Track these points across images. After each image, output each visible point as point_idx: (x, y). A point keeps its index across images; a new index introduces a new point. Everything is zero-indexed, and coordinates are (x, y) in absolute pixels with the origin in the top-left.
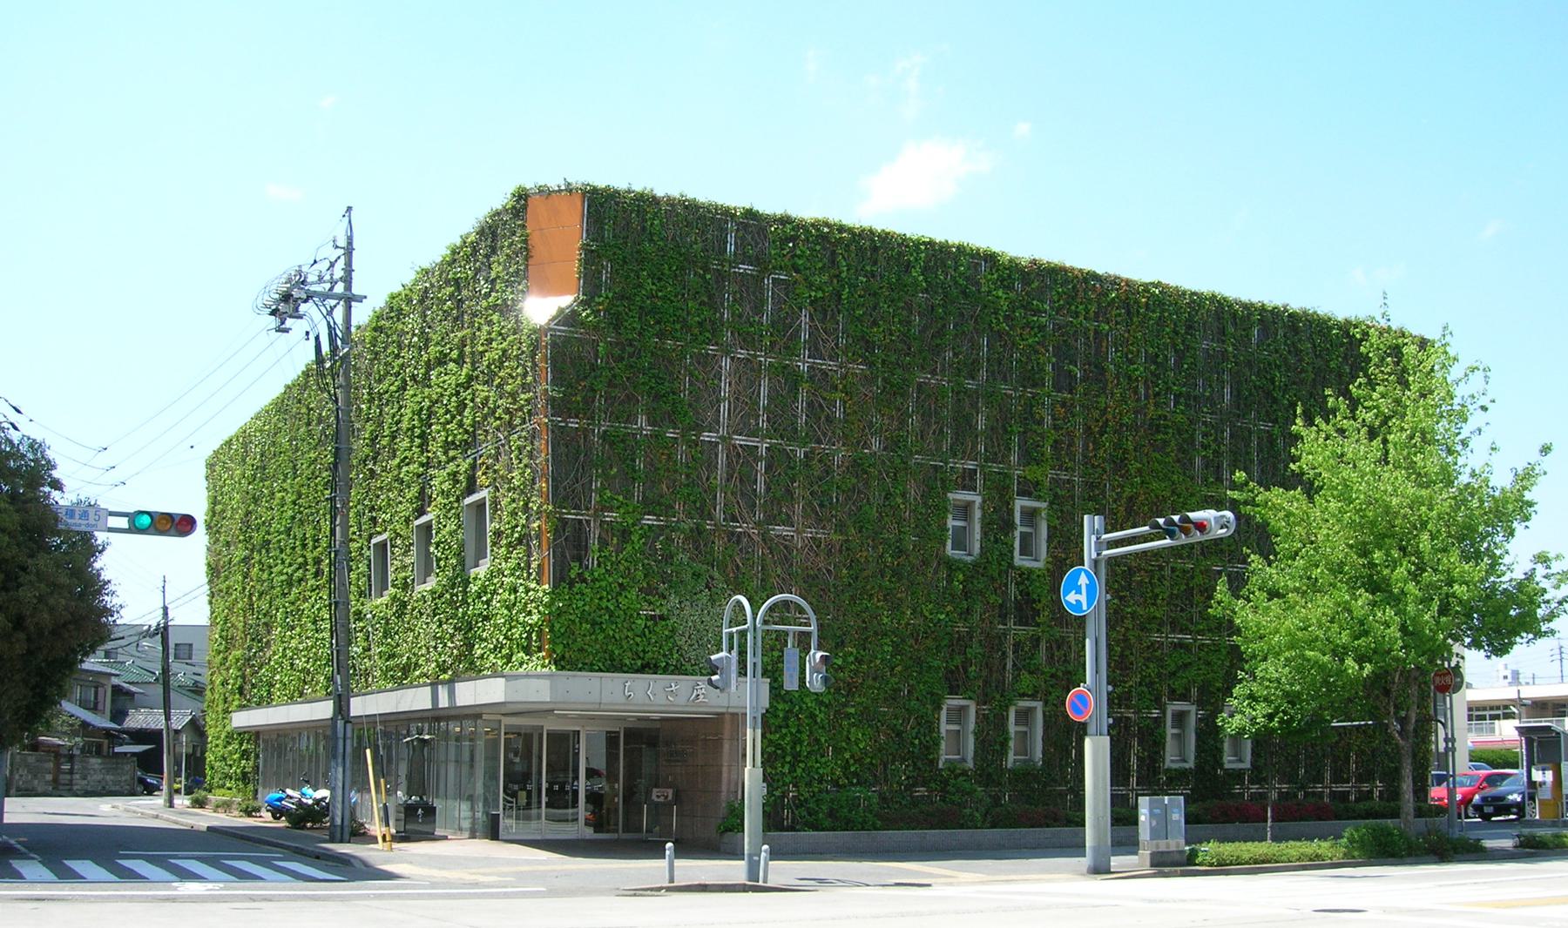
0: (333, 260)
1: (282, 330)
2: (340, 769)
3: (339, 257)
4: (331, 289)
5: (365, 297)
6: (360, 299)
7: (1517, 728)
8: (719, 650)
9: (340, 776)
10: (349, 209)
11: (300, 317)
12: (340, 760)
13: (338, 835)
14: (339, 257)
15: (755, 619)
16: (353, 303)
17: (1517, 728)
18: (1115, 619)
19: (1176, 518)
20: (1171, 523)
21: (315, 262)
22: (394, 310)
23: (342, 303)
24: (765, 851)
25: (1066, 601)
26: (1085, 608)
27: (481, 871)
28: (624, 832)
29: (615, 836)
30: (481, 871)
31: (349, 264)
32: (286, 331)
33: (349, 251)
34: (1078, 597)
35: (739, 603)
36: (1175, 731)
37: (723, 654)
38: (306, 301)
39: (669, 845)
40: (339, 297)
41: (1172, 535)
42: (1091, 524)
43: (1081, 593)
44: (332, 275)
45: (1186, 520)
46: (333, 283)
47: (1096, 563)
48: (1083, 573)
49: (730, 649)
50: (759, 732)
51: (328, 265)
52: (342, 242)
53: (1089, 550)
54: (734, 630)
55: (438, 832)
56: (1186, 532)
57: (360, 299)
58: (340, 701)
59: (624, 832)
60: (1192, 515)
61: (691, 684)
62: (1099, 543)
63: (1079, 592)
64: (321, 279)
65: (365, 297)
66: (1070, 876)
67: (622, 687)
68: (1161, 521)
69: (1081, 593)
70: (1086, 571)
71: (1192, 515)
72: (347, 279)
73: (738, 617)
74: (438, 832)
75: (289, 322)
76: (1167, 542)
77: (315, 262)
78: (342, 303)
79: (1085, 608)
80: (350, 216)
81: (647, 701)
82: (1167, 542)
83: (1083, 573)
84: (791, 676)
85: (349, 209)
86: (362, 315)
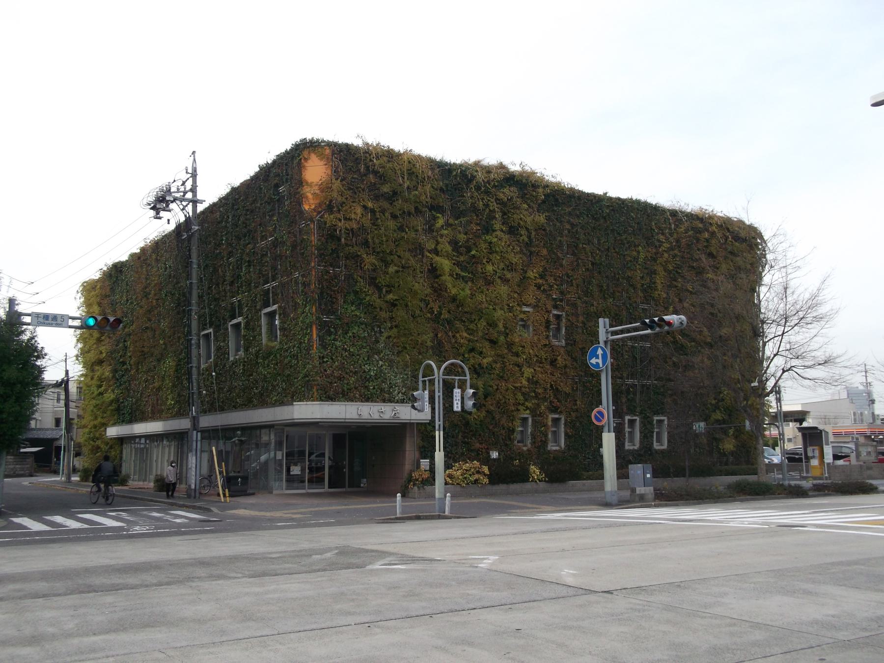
0: (184, 180)
1: (157, 217)
2: (194, 458)
3: (188, 179)
4: (184, 196)
5: (205, 201)
6: (202, 202)
7: (798, 428)
8: (417, 390)
9: (194, 461)
10: (194, 153)
11: (170, 211)
12: (194, 453)
13: (193, 494)
14: (188, 179)
15: (439, 374)
16: (198, 204)
17: (798, 428)
18: (616, 369)
19: (656, 319)
20: (653, 321)
21: (175, 181)
22: (213, 208)
23: (191, 204)
24: (449, 496)
25: (590, 363)
26: (601, 366)
27: (292, 511)
28: (349, 487)
29: (344, 490)
30: (292, 511)
31: (194, 182)
32: (160, 218)
33: (194, 175)
34: (597, 360)
35: (429, 366)
36: (630, 430)
37: (419, 392)
38: (172, 202)
39: (399, 495)
40: (190, 201)
41: (652, 328)
42: (603, 323)
43: (598, 359)
44: (185, 188)
45: (661, 320)
46: (185, 193)
47: (606, 342)
48: (599, 349)
49: (424, 389)
50: (442, 433)
51: (182, 182)
52: (190, 171)
53: (602, 337)
54: (426, 379)
55: (249, 491)
56: (660, 326)
57: (202, 202)
58: (194, 421)
59: (349, 487)
60: (665, 317)
61: (393, 407)
62: (607, 332)
63: (597, 357)
64: (178, 191)
65: (205, 201)
66: (597, 507)
67: (357, 410)
68: (647, 321)
69: (598, 359)
70: (601, 348)
71: (665, 317)
72: (194, 190)
73: (429, 371)
74: (249, 491)
75: (162, 214)
76: (649, 331)
77: (175, 181)
78: (191, 204)
79: (601, 366)
80: (194, 156)
81: (370, 418)
82: (649, 331)
83: (599, 349)
84: (457, 404)
85: (194, 153)
86: (200, 208)
